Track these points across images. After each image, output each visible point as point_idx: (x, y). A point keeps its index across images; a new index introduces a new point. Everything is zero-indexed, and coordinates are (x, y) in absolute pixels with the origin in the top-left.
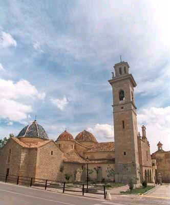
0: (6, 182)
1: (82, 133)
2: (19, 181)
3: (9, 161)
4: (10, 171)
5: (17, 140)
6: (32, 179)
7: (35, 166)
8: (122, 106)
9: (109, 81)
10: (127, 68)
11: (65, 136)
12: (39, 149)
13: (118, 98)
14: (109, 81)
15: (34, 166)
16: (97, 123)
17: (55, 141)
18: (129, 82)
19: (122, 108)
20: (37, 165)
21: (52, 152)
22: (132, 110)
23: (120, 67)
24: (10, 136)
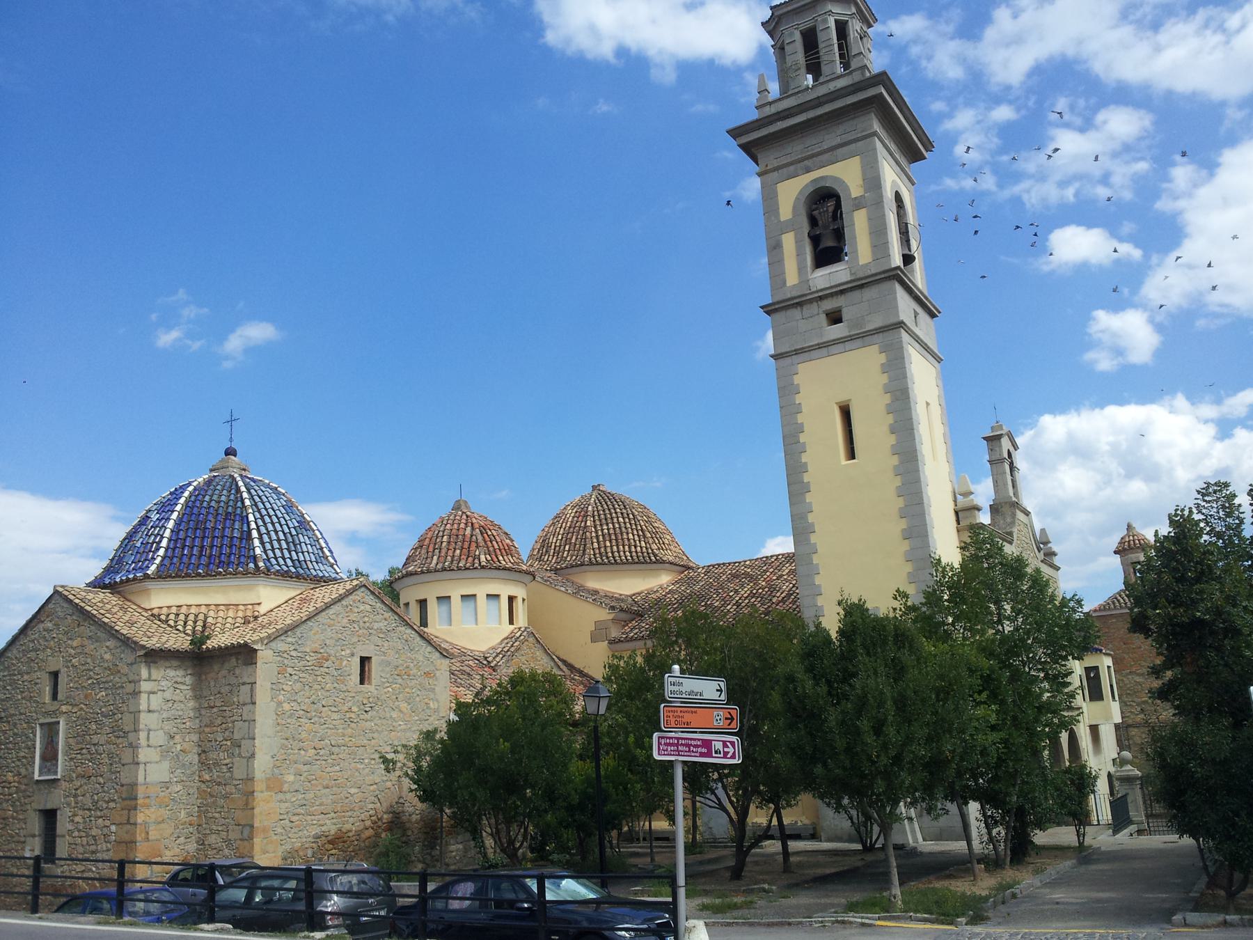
0: (34, 909)
1: (581, 510)
2: (28, 883)
3: (50, 757)
4: (63, 825)
5: (103, 604)
6: (122, 864)
7: (250, 779)
8: (829, 305)
9: (735, 133)
10: (855, 26)
11: (455, 537)
12: (265, 655)
13: (794, 248)
14: (735, 133)
15: (239, 773)
16: (1041, 414)
17: (401, 567)
18: (877, 126)
19: (835, 318)
20: (262, 765)
21: (364, 661)
22: (901, 325)
23: (805, 21)
24: (1172, 522)
